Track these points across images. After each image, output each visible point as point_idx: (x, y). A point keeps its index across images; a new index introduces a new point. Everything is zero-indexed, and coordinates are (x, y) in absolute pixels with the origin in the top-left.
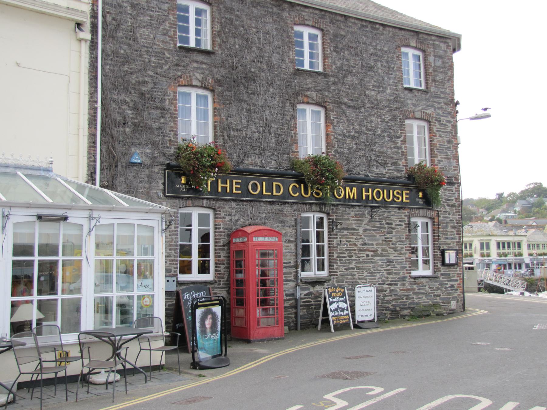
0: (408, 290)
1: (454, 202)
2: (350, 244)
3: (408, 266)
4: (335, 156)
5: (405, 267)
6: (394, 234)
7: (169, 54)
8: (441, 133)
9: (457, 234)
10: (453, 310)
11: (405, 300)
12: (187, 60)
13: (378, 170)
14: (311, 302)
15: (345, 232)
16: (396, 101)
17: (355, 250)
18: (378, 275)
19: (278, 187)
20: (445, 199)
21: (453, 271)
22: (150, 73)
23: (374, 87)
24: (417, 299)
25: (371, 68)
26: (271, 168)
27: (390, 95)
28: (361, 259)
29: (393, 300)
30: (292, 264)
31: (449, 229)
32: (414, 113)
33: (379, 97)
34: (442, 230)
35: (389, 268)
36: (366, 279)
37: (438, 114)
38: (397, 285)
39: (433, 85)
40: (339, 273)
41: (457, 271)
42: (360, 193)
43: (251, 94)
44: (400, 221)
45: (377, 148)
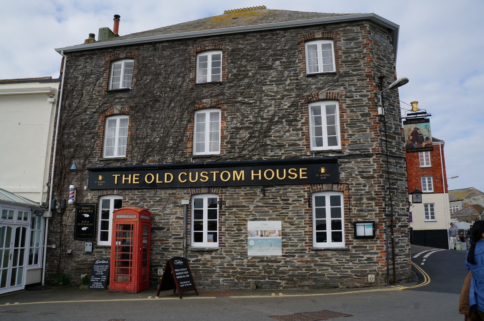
0: (307, 262)
1: (371, 173)
2: (239, 220)
3: (307, 238)
6: (291, 209)
7: (101, 98)
8: (352, 108)
9: (375, 206)
10: (371, 283)
11: (304, 271)
12: (111, 99)
13: (273, 153)
14: (199, 267)
15: (234, 209)
21: (369, 244)
23: (271, 81)
24: (319, 270)
29: (289, 270)
30: (181, 236)
34: (355, 202)
37: (350, 91)
38: (294, 256)
40: (227, 245)
41: (376, 244)
42: (248, 175)
43: (155, 111)
44: (298, 197)
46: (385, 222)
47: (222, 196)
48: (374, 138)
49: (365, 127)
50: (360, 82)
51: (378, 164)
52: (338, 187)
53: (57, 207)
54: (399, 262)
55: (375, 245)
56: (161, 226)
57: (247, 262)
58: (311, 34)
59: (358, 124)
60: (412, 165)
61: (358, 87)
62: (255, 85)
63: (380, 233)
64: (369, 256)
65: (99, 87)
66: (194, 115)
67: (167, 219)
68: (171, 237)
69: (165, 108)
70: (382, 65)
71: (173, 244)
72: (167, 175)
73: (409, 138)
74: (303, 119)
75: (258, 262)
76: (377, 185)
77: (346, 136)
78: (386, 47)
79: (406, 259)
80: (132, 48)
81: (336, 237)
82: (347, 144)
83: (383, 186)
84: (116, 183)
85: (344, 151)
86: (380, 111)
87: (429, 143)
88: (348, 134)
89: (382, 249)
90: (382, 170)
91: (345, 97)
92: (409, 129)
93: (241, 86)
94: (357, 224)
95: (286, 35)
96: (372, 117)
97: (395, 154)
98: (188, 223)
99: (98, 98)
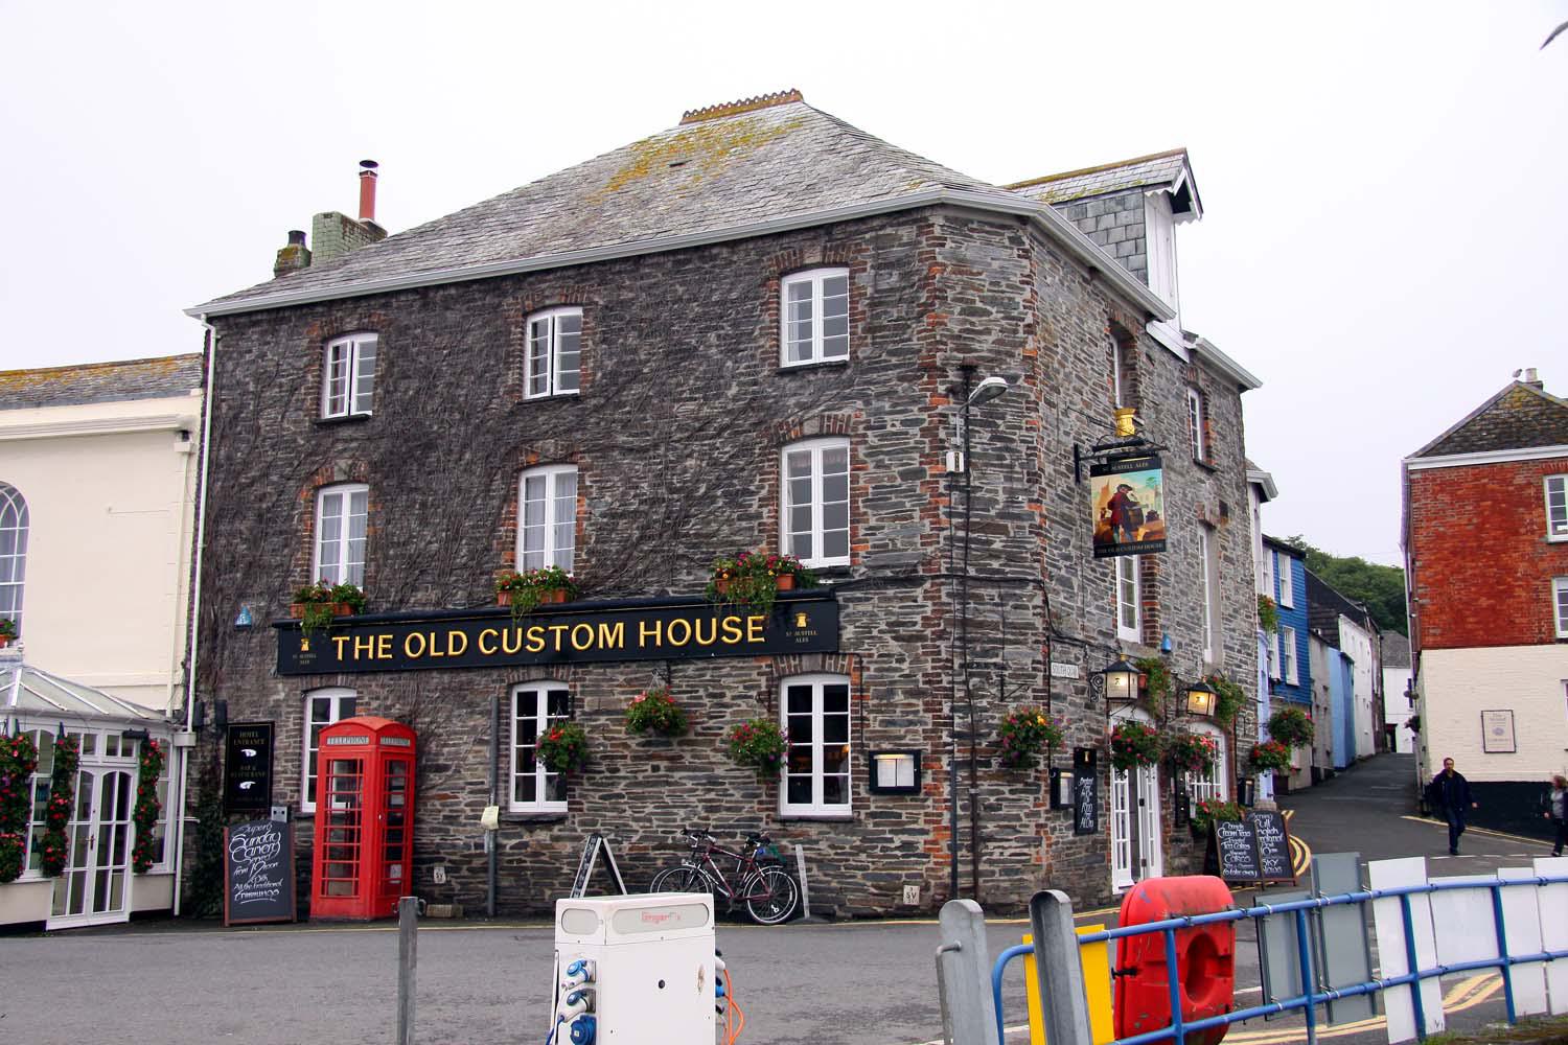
1: (918, 627)
2: (612, 745)
4: (588, 561)
5: (757, 796)
6: (728, 718)
8: (881, 457)
9: (925, 711)
13: (691, 578)
14: (525, 862)
15: (603, 720)
16: (753, 409)
17: (625, 757)
18: (682, 813)
19: (457, 639)
20: (887, 624)
21: (907, 807)
22: (275, 478)
23: (692, 391)
25: (690, 353)
26: (455, 605)
27: (735, 399)
28: (640, 776)
30: (486, 787)
31: (899, 698)
32: (801, 424)
33: (706, 410)
34: (875, 702)
35: (712, 795)
36: (650, 821)
37: (879, 412)
38: (733, 835)
39: (869, 341)
40: (585, 806)
41: (923, 807)
42: (631, 634)
43: (430, 473)
44: (745, 687)
45: (692, 527)
46: (952, 752)
47: (575, 686)
48: (930, 536)
49: (908, 505)
50: (906, 384)
51: (934, 604)
52: (836, 663)
53: (207, 720)
54: (996, 856)
55: (922, 811)
56: (441, 761)
57: (630, 849)
58: (795, 254)
59: (894, 500)
60: (1517, 533)
61: (900, 398)
62: (655, 401)
63: (934, 779)
64: (905, 838)
65: (297, 410)
66: (517, 482)
67: (454, 745)
68: (463, 789)
69: (451, 465)
70: (981, 328)
71: (466, 805)
72: (455, 636)
73: (1103, 516)
74: (763, 487)
75: (654, 848)
76: (929, 659)
77: (862, 532)
78: (1003, 273)
79: (1026, 850)
80: (373, 303)
81: (833, 791)
82: (862, 553)
83: (947, 660)
84: (340, 657)
85: (856, 571)
86: (952, 461)
87: (1156, 528)
88: (866, 525)
89: (939, 822)
90: (946, 620)
91: (865, 429)
92: (1106, 489)
93: (622, 404)
94: (876, 757)
95: (735, 258)
96: (928, 479)
97: (1003, 572)
98: (500, 755)
99: (295, 441)
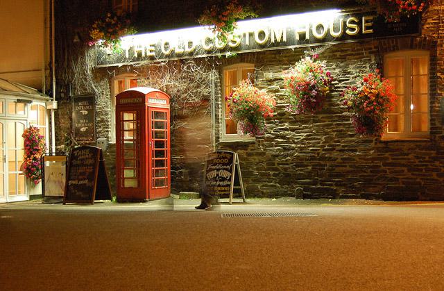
29: (348, 172)
